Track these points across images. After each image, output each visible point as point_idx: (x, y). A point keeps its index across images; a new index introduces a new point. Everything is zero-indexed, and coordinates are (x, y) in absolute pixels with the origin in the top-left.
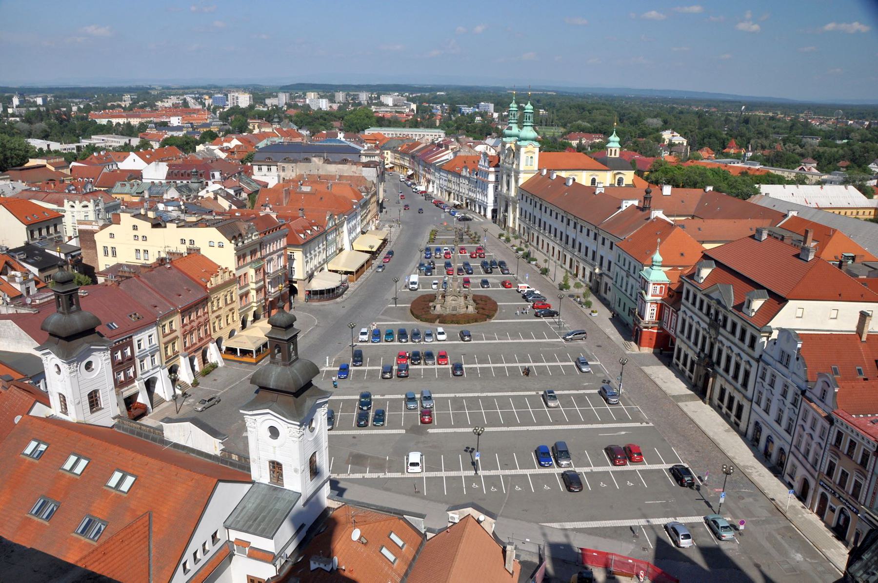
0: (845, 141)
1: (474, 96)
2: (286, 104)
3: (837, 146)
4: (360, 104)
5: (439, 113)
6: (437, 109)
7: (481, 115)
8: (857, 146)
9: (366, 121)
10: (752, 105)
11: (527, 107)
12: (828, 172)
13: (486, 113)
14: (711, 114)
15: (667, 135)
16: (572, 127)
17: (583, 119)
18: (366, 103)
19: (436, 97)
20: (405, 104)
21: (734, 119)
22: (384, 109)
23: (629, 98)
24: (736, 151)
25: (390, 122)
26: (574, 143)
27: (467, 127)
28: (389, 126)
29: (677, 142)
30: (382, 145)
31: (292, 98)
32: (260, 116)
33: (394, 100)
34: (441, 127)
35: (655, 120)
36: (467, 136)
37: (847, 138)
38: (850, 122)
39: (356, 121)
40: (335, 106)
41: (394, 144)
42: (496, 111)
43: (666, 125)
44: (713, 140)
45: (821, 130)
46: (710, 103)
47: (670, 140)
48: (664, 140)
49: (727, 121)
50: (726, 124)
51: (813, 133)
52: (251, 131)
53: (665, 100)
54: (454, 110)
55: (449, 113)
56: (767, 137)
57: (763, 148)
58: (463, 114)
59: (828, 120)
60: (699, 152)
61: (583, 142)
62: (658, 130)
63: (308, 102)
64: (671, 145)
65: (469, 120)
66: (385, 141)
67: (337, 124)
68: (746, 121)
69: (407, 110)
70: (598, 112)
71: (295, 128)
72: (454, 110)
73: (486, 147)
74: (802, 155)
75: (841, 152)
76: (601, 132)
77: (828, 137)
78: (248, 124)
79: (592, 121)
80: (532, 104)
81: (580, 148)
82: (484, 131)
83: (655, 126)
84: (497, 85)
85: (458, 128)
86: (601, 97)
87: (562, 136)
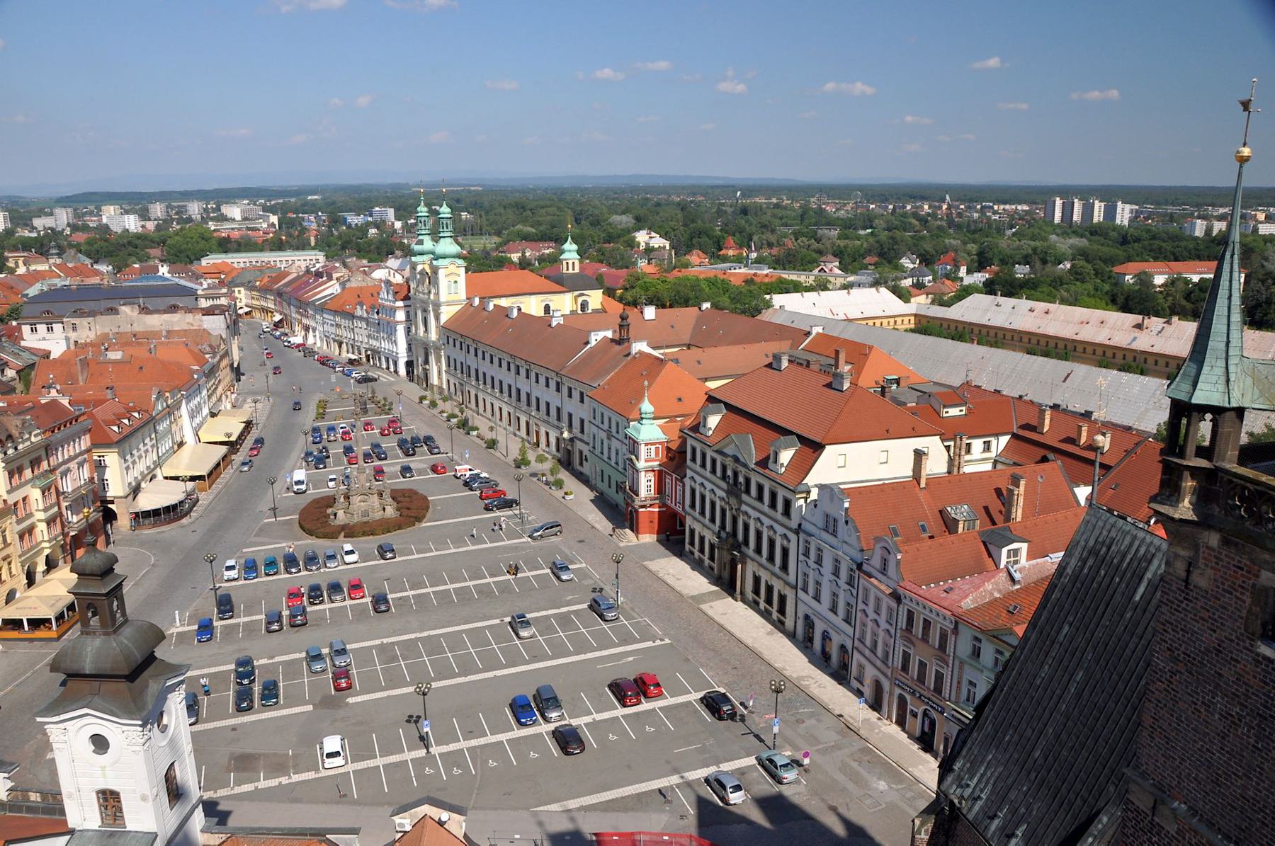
1: (364, 200)
2: (69, 225)
4: (190, 220)
5: (314, 226)
6: (309, 221)
7: (377, 227)
8: (884, 236)
9: (202, 244)
10: (749, 191)
11: (442, 210)
12: (854, 273)
13: (384, 222)
14: (698, 204)
15: (642, 237)
17: (524, 221)
18: (199, 217)
19: (306, 204)
20: (261, 217)
21: (729, 210)
22: (228, 225)
23: (586, 189)
24: (736, 252)
25: (239, 244)
26: (515, 257)
27: (358, 244)
28: (238, 251)
30: (230, 281)
31: (77, 215)
32: (26, 245)
33: (243, 212)
34: (317, 247)
36: (359, 258)
39: (186, 247)
40: (151, 226)
41: (248, 277)
42: (397, 218)
43: (640, 223)
44: (704, 239)
45: (838, 218)
46: (694, 190)
47: (647, 244)
48: (639, 243)
49: (720, 213)
51: (830, 223)
52: (12, 271)
53: (634, 190)
54: (335, 221)
55: (329, 227)
56: (773, 231)
57: (770, 245)
58: (349, 226)
59: (845, 205)
62: (629, 231)
63: (105, 220)
64: (649, 250)
65: (359, 234)
66: (234, 274)
67: (155, 252)
68: (745, 211)
69: (265, 225)
70: (544, 211)
71: (88, 261)
72: (335, 221)
73: (389, 272)
74: (820, 252)
75: (865, 245)
76: (551, 240)
77: (848, 226)
78: (7, 259)
79: (536, 224)
81: (524, 264)
82: (383, 249)
83: (623, 226)
84: (396, 181)
85: (344, 248)
86: (546, 190)
87: (497, 249)
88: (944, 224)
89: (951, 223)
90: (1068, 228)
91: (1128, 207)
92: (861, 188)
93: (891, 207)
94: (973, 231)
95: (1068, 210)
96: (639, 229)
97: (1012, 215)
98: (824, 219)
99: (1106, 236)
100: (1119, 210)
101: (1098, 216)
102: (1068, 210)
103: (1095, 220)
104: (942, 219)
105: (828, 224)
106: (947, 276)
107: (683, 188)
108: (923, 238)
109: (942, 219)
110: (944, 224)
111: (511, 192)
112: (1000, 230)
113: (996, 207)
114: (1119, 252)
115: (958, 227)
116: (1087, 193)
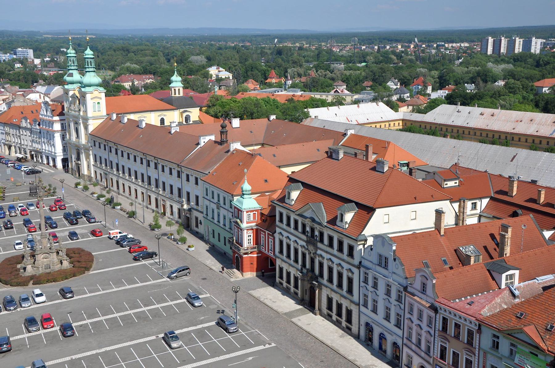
0: (364, 64)
7: (21, 62)
8: (375, 67)
10: (282, 38)
11: (69, 51)
12: (357, 93)
15: (213, 71)
16: (121, 70)
17: (131, 60)
21: (269, 52)
24: (277, 81)
26: (127, 85)
29: (223, 77)
35: (199, 58)
36: (11, 84)
37: (365, 62)
38: (364, 47)
42: (36, 56)
43: (211, 61)
45: (342, 56)
46: (243, 38)
47: (217, 76)
48: (211, 75)
49: (263, 54)
50: (262, 57)
51: (337, 59)
53: (203, 39)
56: (301, 66)
57: (300, 75)
59: (345, 47)
60: (245, 84)
61: (136, 83)
62: (204, 67)
64: (219, 80)
65: (9, 68)
68: (279, 52)
73: (37, 95)
74: (333, 79)
75: (363, 74)
77: (349, 60)
79: (138, 62)
80: (74, 49)
81: (134, 91)
82: (28, 79)
87: (113, 79)
88: (413, 58)
89: (418, 58)
90: (498, 58)
91: (540, 41)
92: (355, 35)
93: (376, 47)
95: (497, 45)
96: (211, 66)
97: (458, 51)
99: (525, 61)
100: (533, 43)
101: (518, 48)
102: (497, 45)
103: (516, 51)
104: (411, 55)
105: (336, 60)
106: (419, 93)
107: (235, 37)
108: (401, 68)
109: (411, 55)
110: (413, 58)
111: (117, 39)
112: (451, 60)
113: (446, 45)
114: (536, 72)
115: (423, 60)
116: (510, 33)
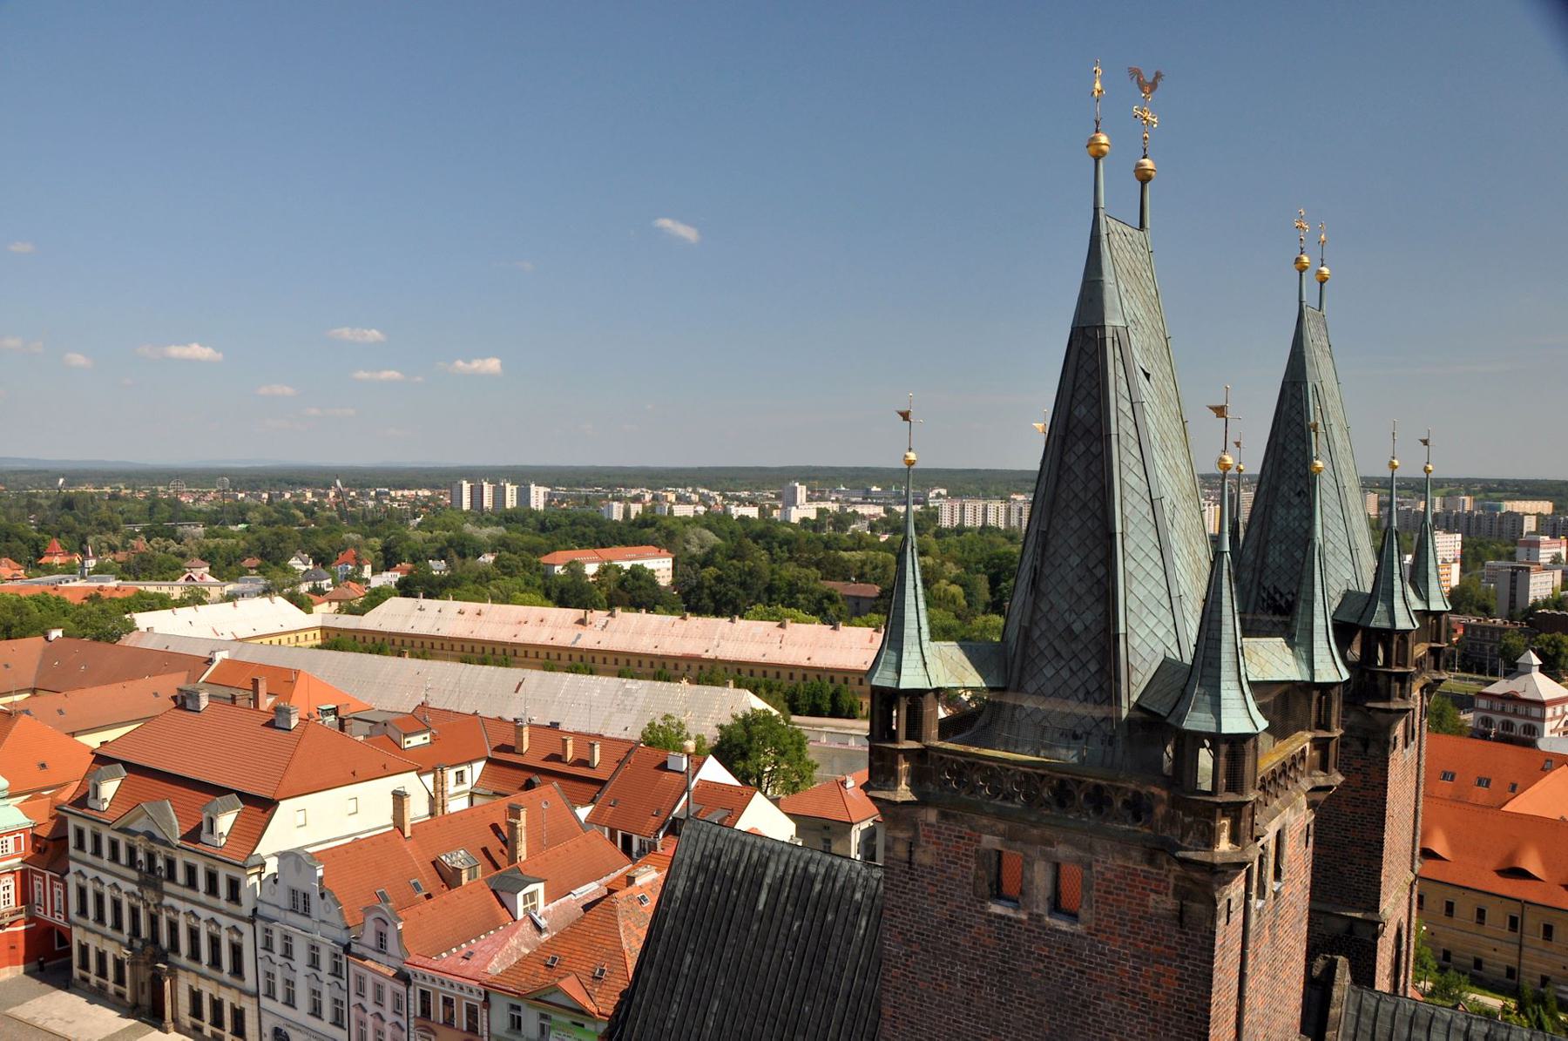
3: (232, 535)
8: (265, 532)
10: (74, 477)
12: (231, 580)
24: (65, 560)
37: (244, 521)
38: (241, 495)
45: (200, 511)
49: (32, 506)
50: (31, 512)
51: (191, 517)
56: (115, 530)
57: (113, 549)
59: (205, 494)
68: (69, 504)
74: (182, 555)
75: (242, 544)
77: (214, 519)
88: (335, 514)
89: (343, 514)
90: (479, 515)
91: (542, 490)
92: (223, 473)
93: (265, 496)
94: (372, 524)
95: (477, 494)
97: (414, 502)
98: (181, 514)
99: (523, 522)
100: (533, 494)
101: (511, 502)
102: (477, 494)
103: (508, 506)
104: (331, 509)
105: (187, 519)
106: (347, 578)
108: (314, 532)
109: (331, 509)
110: (335, 514)
112: (403, 521)
114: (541, 540)
115: (353, 519)
116: (497, 476)
